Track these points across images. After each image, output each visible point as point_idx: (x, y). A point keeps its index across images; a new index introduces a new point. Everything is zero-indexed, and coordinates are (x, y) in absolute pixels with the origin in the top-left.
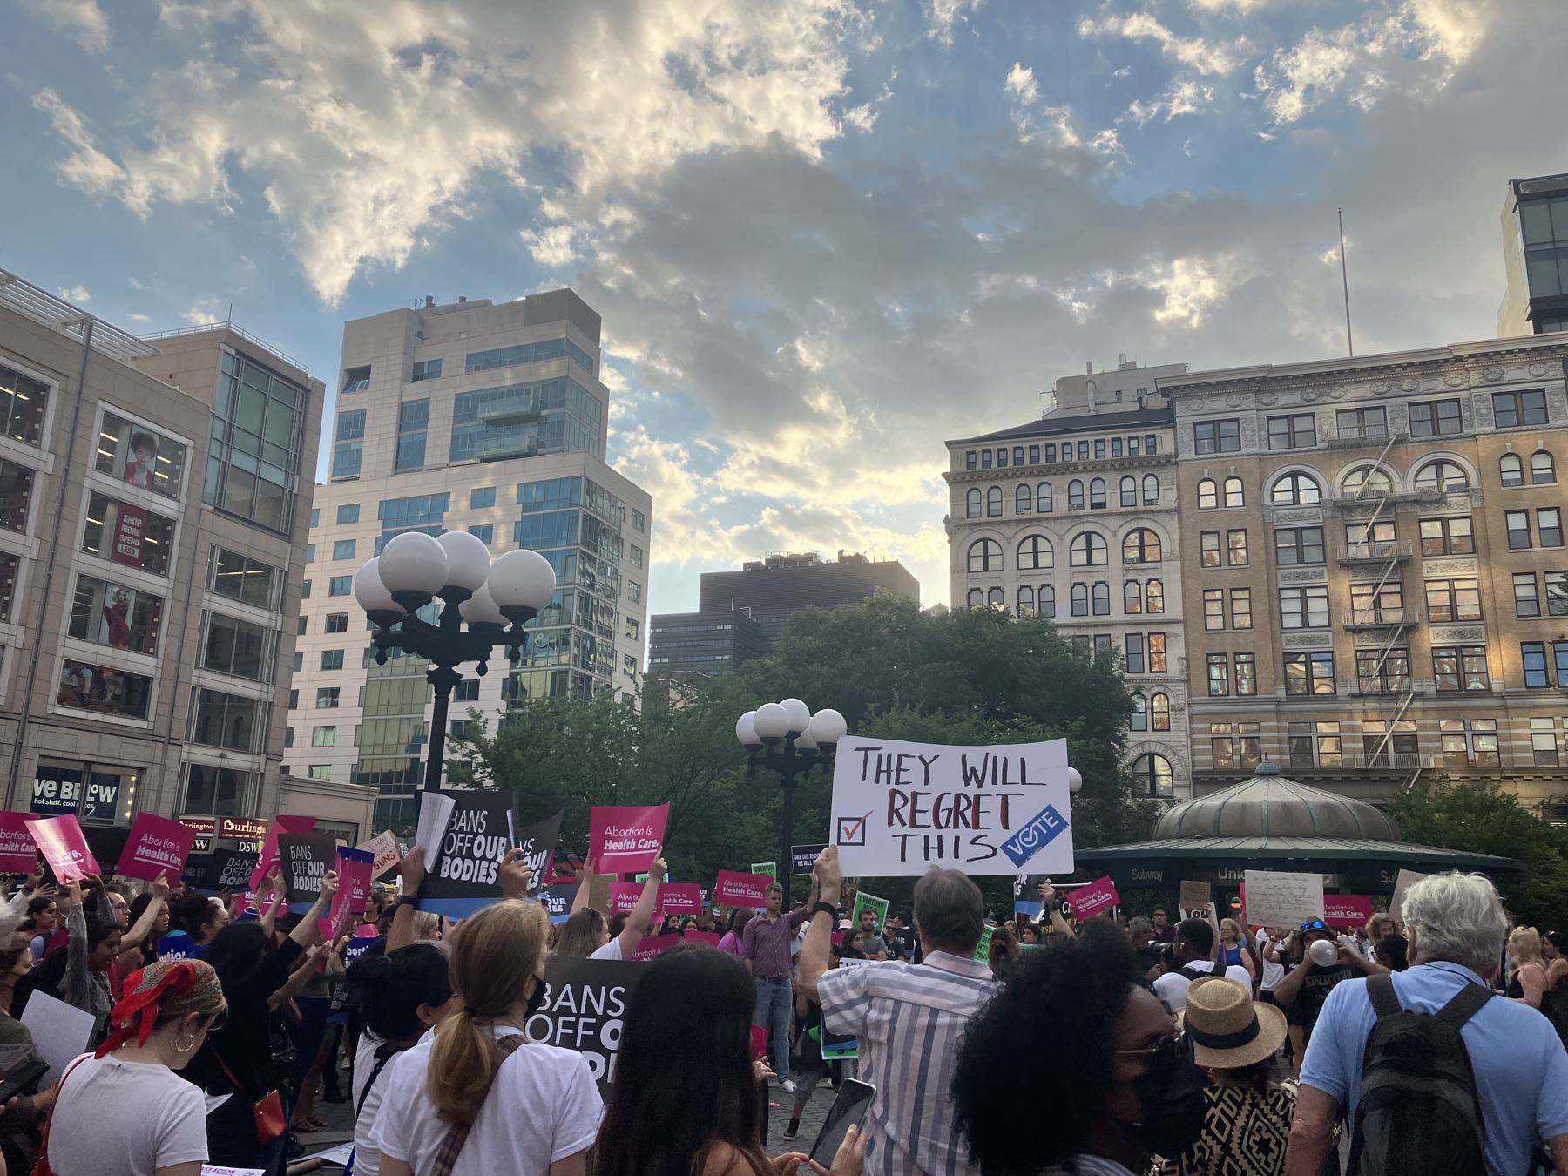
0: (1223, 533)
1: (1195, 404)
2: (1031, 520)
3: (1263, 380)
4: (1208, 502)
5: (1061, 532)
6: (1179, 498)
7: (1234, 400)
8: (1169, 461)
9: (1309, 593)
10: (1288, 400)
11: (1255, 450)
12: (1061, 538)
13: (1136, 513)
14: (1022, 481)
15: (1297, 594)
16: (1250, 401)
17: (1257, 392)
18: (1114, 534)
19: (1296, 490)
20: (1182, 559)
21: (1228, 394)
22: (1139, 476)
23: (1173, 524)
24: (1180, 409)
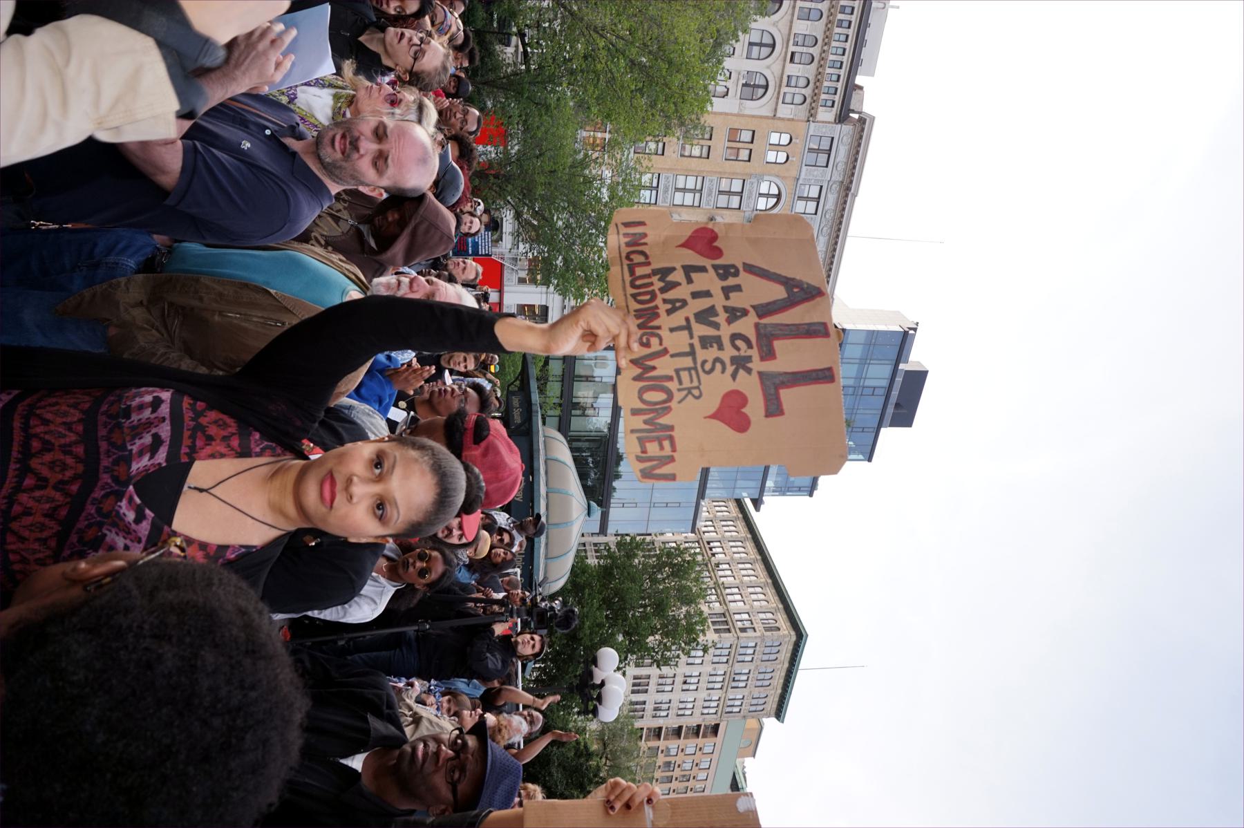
0: (751, 146)
1: (847, 140)
3: (848, 189)
4: (774, 138)
5: (780, 25)
6: (783, 119)
7: (841, 167)
8: (812, 115)
9: (698, 195)
10: (830, 201)
11: (803, 176)
12: (775, 24)
13: (780, 86)
15: (698, 187)
16: (837, 177)
18: (768, 67)
19: (768, 196)
20: (738, 115)
21: (846, 163)
22: (808, 92)
24: (847, 128)
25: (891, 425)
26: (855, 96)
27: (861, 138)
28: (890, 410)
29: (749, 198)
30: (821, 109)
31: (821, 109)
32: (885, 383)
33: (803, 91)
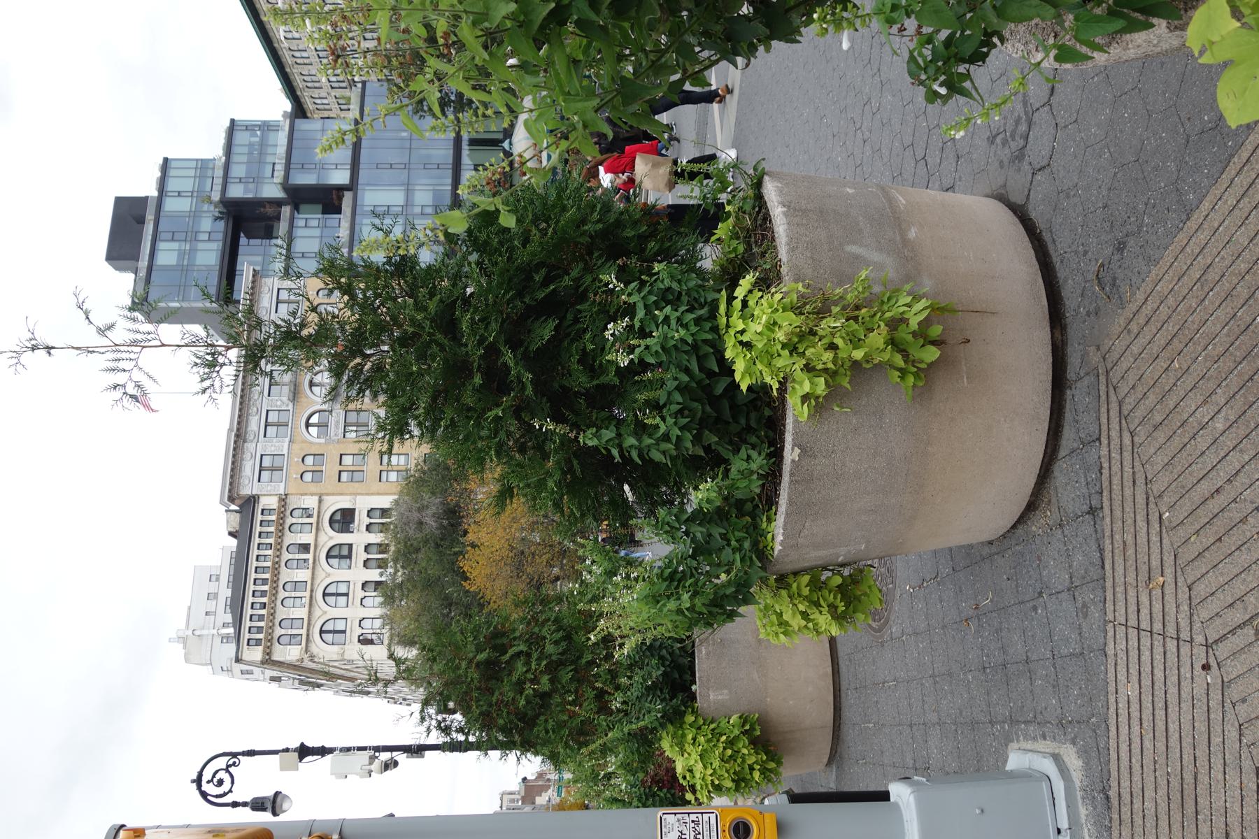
0: (341, 468)
1: (244, 481)
2: (311, 597)
3: (237, 436)
5: (323, 575)
7: (247, 456)
8: (283, 500)
10: (254, 424)
12: (328, 575)
14: (279, 602)
16: (250, 447)
17: (245, 441)
18: (331, 538)
21: (242, 459)
23: (328, 500)
24: (246, 491)
25: (147, 198)
26: (235, 525)
27: (231, 484)
28: (150, 217)
29: (338, 422)
30: (275, 506)
31: (275, 506)
32: (161, 245)
33: (294, 521)
